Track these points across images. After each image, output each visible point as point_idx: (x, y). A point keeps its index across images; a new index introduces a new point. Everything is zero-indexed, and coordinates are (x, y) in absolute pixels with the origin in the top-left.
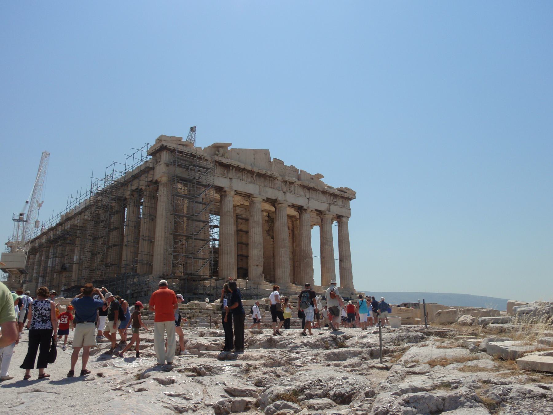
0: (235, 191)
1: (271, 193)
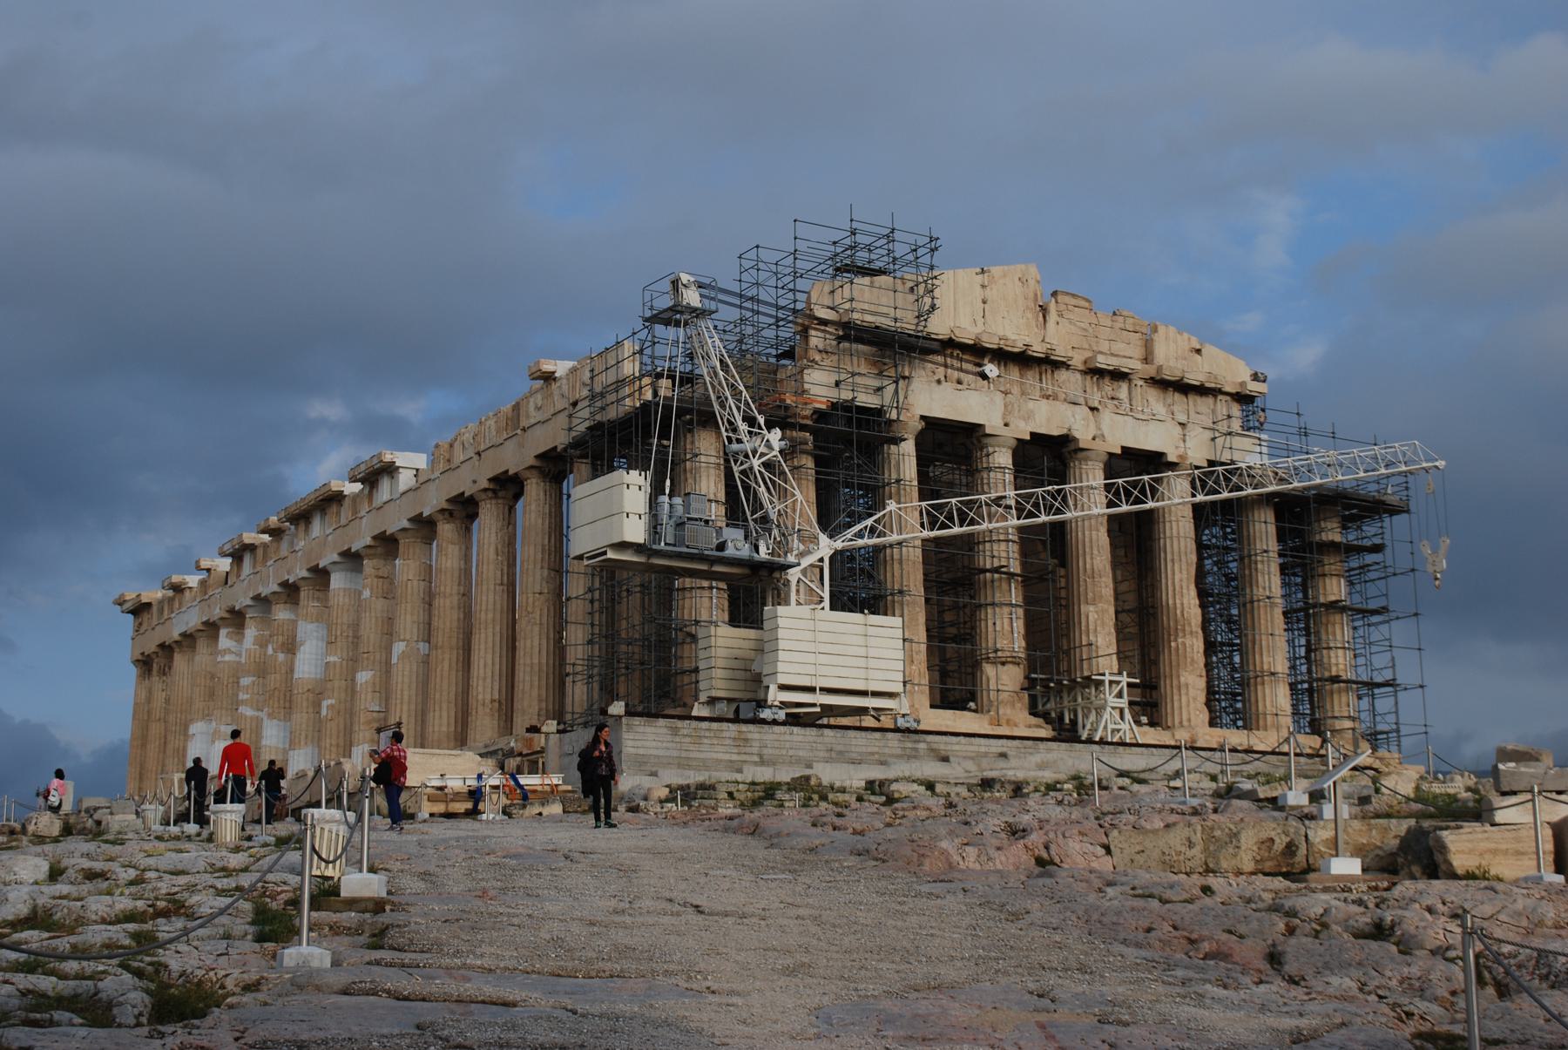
0: (922, 417)
1: (1046, 418)
